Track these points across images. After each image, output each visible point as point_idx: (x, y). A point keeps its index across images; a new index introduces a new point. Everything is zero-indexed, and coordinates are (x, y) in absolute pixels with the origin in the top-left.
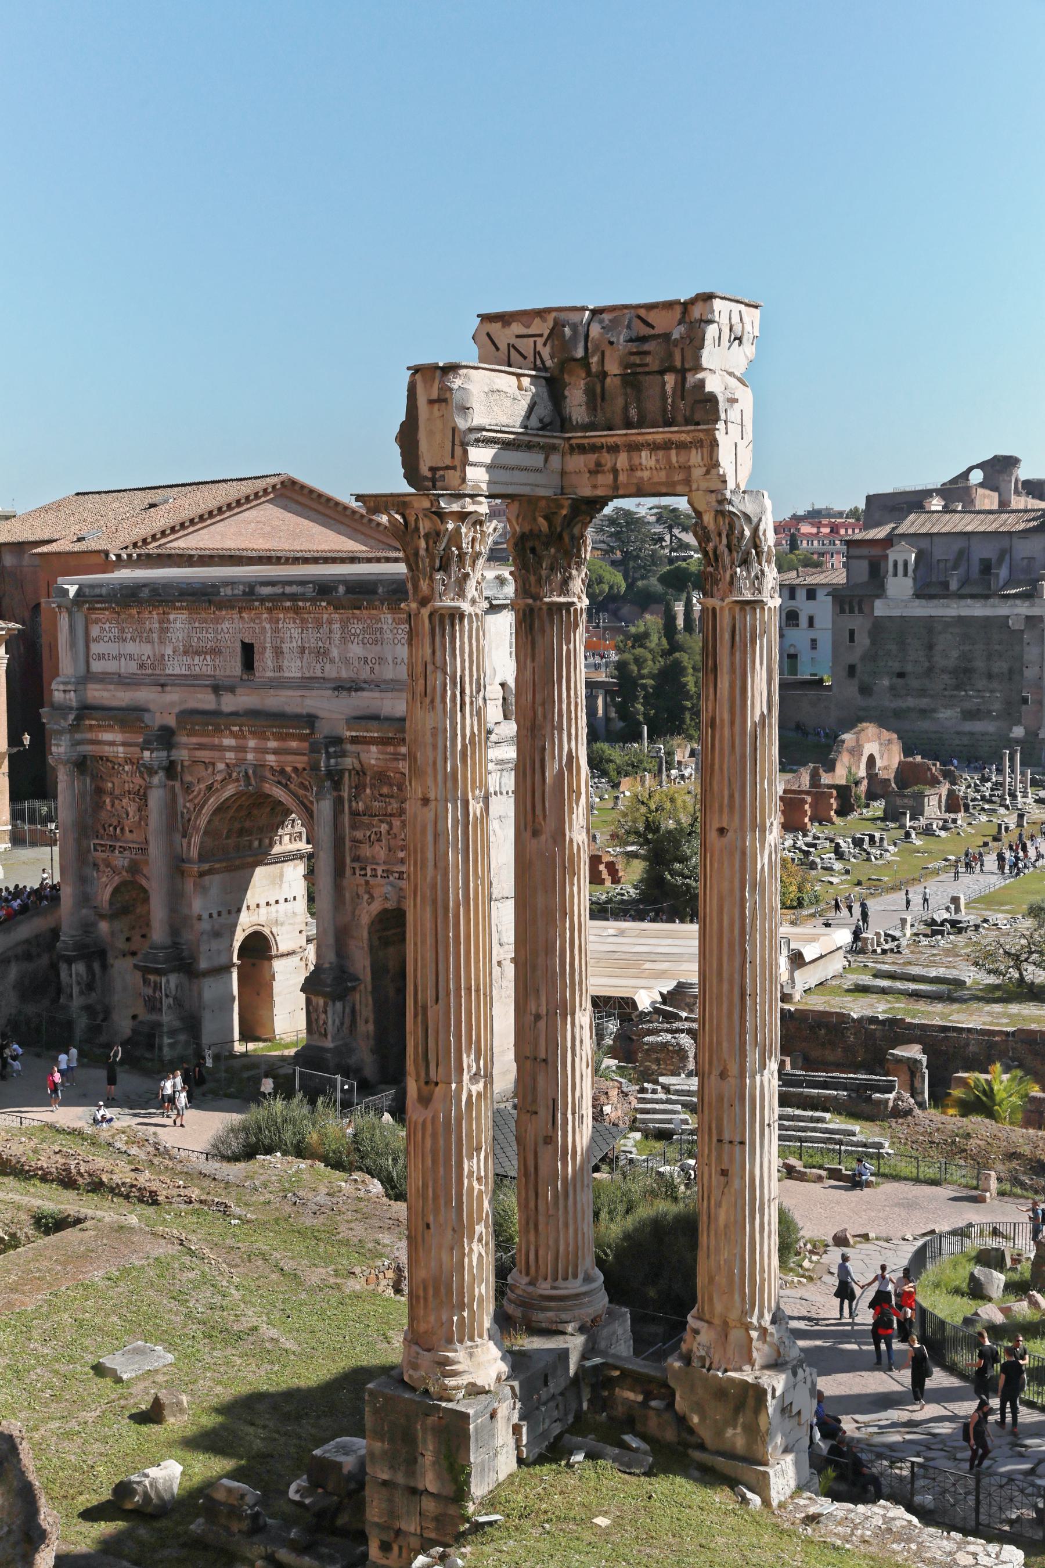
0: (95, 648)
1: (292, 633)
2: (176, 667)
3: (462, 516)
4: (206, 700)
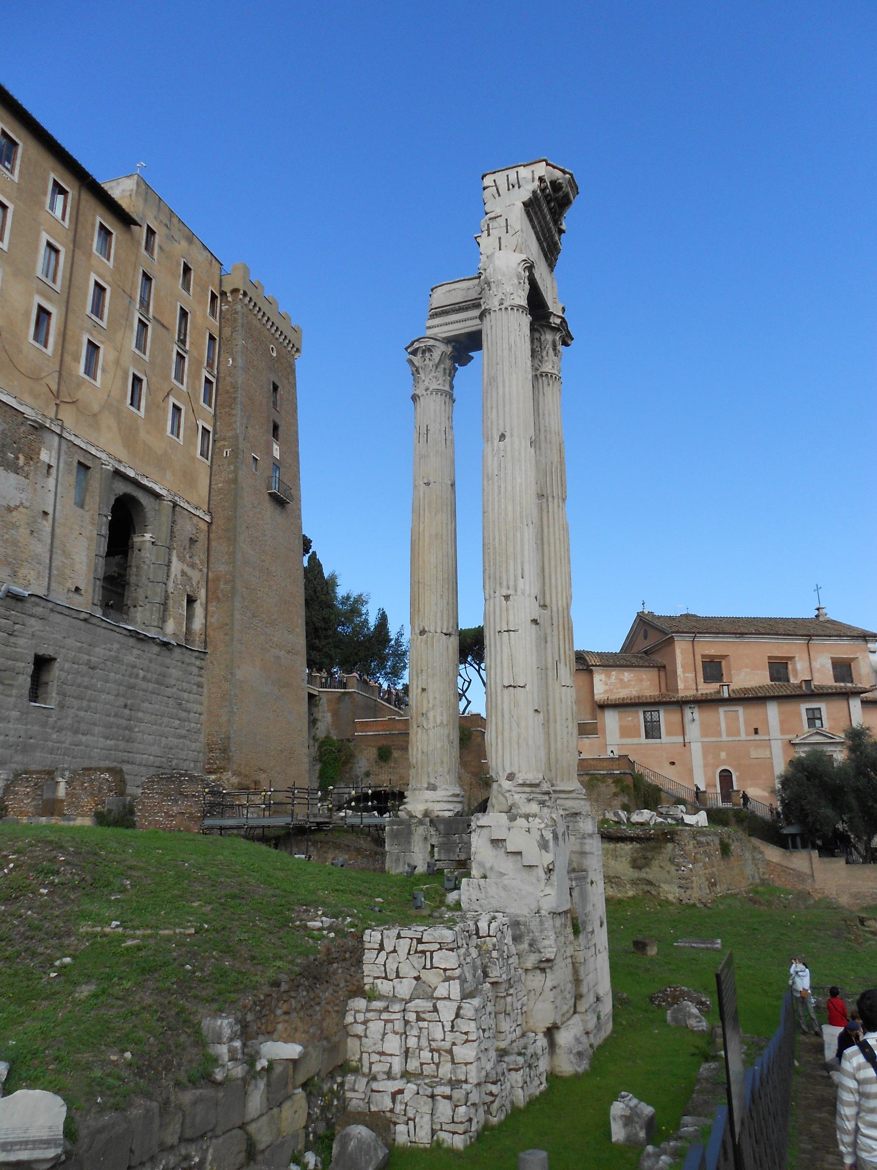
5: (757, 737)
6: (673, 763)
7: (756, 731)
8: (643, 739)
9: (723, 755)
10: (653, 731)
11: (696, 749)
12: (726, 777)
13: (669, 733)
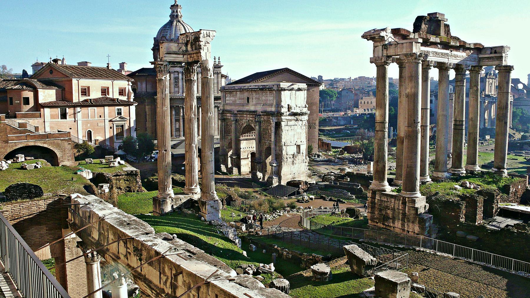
0: (227, 99)
1: (254, 94)
2: (238, 102)
3: (162, 65)
4: (241, 108)
5: (101, 119)
6: (71, 129)
7: (100, 116)
9: (89, 125)
10: (64, 116)
12: (90, 134)
13: (69, 118)
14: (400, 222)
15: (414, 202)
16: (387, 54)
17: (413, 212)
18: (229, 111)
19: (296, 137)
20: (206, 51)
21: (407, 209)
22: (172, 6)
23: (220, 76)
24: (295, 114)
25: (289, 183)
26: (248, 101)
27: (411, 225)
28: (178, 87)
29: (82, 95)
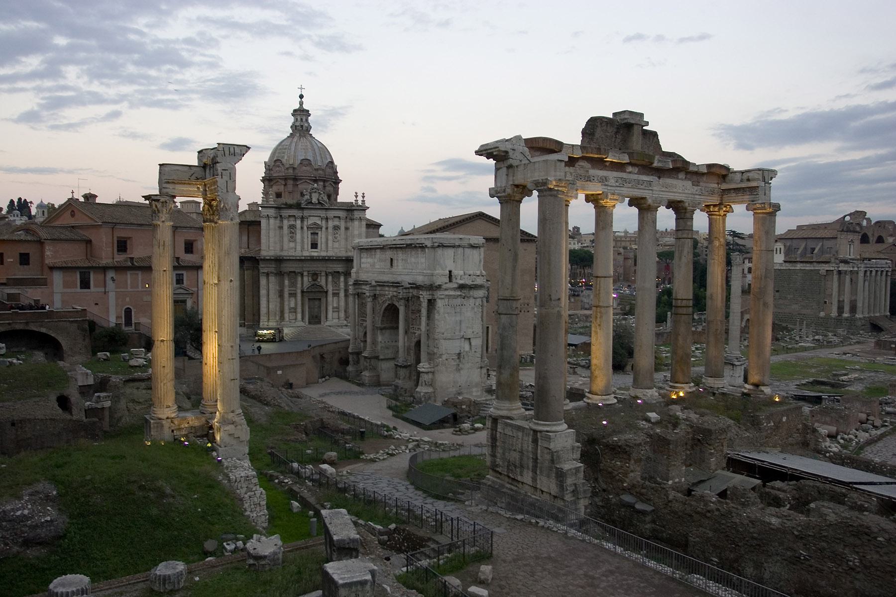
0: (363, 260)
8: (79, 290)
9: (128, 299)
10: (85, 284)
11: (112, 296)
12: (128, 312)
13: (96, 286)
14: (530, 474)
15: (549, 439)
16: (513, 180)
17: (548, 457)
18: (366, 283)
19: (463, 325)
20: (225, 178)
21: (539, 451)
22: (295, 111)
23: (364, 223)
24: (462, 287)
25: (446, 403)
26: (392, 265)
27: (544, 479)
28: (295, 241)
29: (118, 251)
